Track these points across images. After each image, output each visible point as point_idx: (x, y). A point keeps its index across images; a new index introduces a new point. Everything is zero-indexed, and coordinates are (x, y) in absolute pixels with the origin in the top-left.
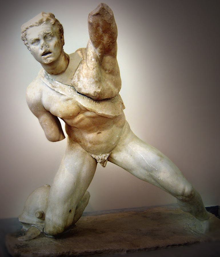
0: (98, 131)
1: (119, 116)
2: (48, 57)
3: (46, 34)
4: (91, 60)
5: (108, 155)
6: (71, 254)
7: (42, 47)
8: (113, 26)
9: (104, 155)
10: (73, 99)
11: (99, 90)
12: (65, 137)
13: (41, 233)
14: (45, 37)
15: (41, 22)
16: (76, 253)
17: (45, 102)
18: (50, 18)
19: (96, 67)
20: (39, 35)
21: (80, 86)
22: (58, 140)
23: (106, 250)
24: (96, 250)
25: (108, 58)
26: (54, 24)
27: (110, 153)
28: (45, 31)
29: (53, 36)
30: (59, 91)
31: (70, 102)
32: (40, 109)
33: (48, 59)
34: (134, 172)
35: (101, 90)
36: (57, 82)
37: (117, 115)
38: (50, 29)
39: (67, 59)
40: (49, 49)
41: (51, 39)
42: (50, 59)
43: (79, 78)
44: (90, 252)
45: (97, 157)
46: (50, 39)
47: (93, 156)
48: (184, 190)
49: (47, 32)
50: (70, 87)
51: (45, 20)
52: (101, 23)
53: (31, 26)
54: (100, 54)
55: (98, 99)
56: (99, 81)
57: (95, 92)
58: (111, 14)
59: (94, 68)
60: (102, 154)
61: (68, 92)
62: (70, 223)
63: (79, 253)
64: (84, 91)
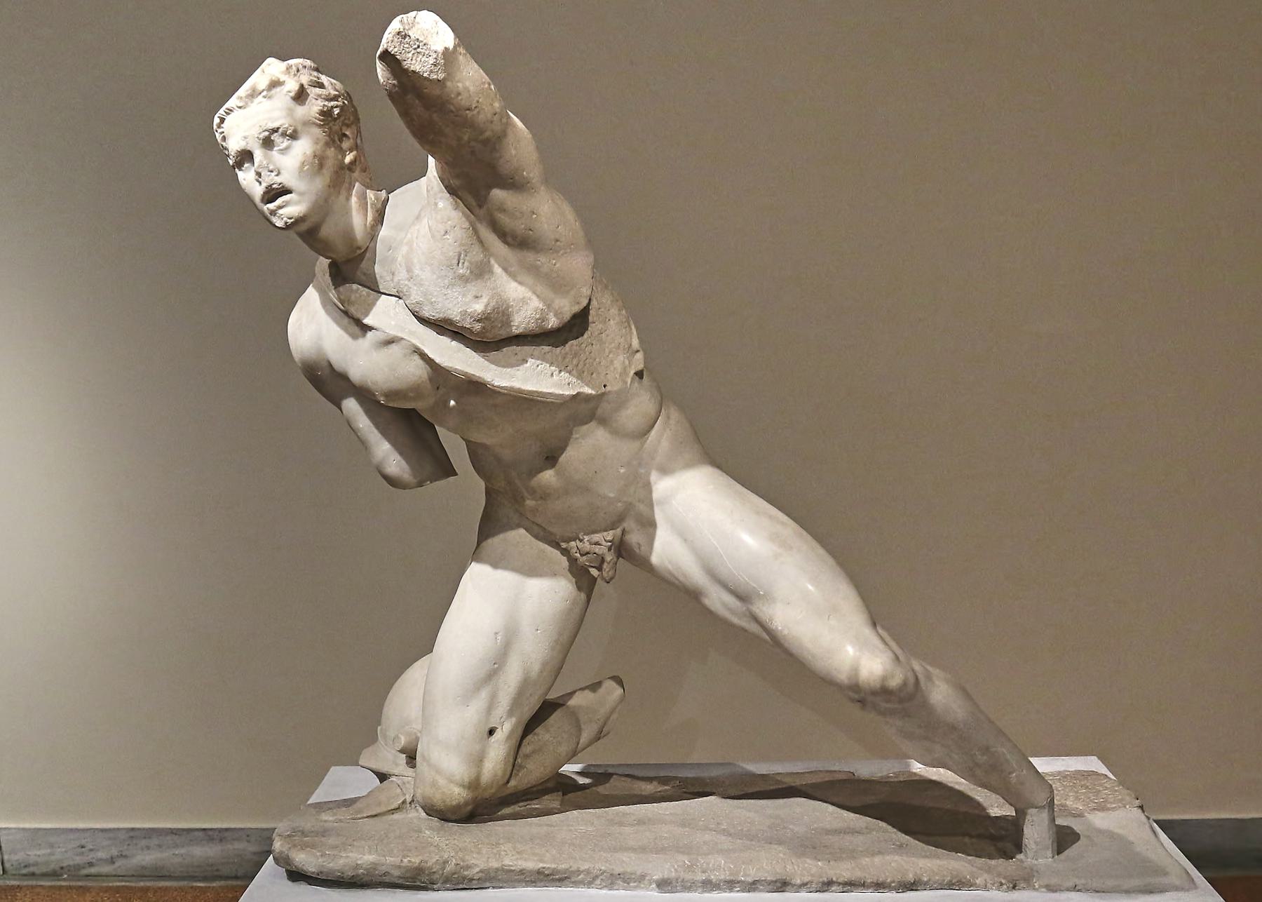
1: (603, 394)
2: (280, 207)
3: (267, 133)
4: (436, 204)
5: (609, 535)
7: (259, 174)
9: (597, 537)
11: (478, 307)
12: (446, 469)
13: (404, 802)
14: (268, 143)
18: (282, 78)
25: (498, 194)
26: (300, 96)
27: (619, 531)
28: (263, 124)
29: (294, 136)
31: (394, 348)
32: (328, 381)
33: (281, 212)
34: (707, 602)
35: (486, 306)
38: (284, 113)
40: (278, 179)
41: (287, 148)
43: (409, 270)
48: (855, 670)
57: (464, 313)
62: (496, 776)
64: (427, 313)
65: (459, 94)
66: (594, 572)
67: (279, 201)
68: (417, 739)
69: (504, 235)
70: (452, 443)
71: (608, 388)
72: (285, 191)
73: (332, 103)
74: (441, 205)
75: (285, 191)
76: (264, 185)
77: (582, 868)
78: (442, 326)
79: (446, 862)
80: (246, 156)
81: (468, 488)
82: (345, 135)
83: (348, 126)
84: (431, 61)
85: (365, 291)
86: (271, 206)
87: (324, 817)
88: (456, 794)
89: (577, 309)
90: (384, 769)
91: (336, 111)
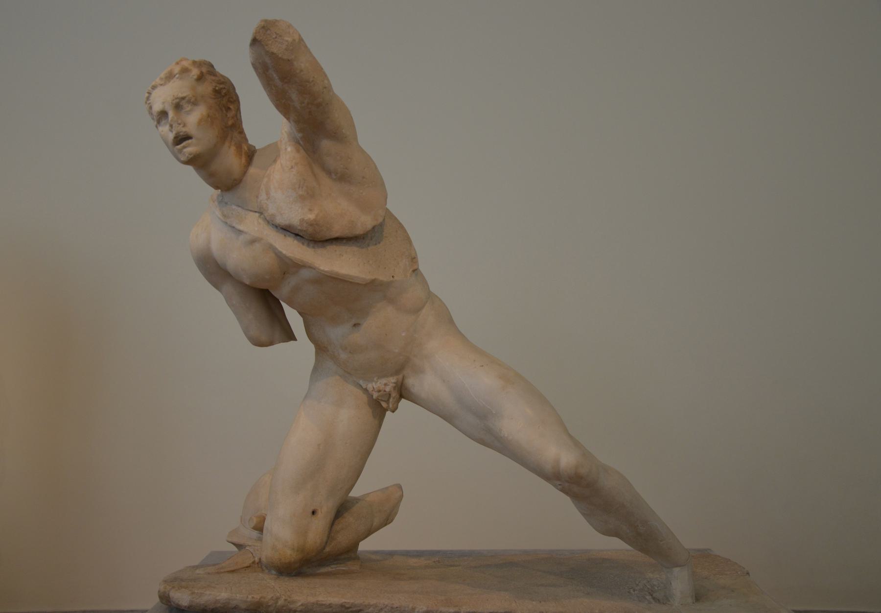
0: (354, 321)
2: (185, 147)
6: (281, 602)
7: (171, 126)
8: (302, 64)
9: (384, 381)
10: (261, 239)
11: (311, 216)
12: (290, 336)
13: (254, 562)
14: (178, 107)
15: (170, 77)
16: (294, 602)
17: (216, 249)
18: (191, 67)
19: (296, 164)
20: (163, 103)
21: (271, 210)
22: (271, 343)
23: (369, 606)
24: (344, 600)
25: (326, 144)
26: (200, 78)
27: (401, 376)
29: (194, 103)
30: (234, 225)
32: (215, 271)
33: (185, 150)
35: (317, 216)
36: (234, 207)
37: (383, 277)
39: (250, 155)
40: (184, 130)
41: (191, 111)
42: (191, 149)
43: (268, 194)
44: (330, 606)
45: (370, 387)
46: (189, 109)
47: (361, 382)
49: (181, 95)
50: (257, 214)
51: (177, 69)
52: (268, 60)
53: (154, 88)
54: (300, 135)
55: (315, 237)
56: (308, 196)
57: (302, 220)
58: (286, 39)
59: (292, 167)
60: (379, 378)
61: (252, 225)
63: (300, 604)
64: (280, 220)
65: (301, 71)
66: (384, 405)
67: (184, 144)
68: (264, 519)
69: (329, 173)
70: (293, 317)
71: (396, 278)
72: (187, 137)
73: (222, 86)
74: (289, 149)
75: (187, 137)
76: (174, 132)
77: (372, 603)
78: (287, 230)
79: (278, 598)
80: (163, 114)
81: (301, 350)
82: (229, 108)
83: (231, 102)
84: (284, 47)
85: (240, 209)
86: (179, 147)
87: (198, 571)
88: (289, 555)
89: (375, 223)
90: (241, 542)
91: (224, 91)
